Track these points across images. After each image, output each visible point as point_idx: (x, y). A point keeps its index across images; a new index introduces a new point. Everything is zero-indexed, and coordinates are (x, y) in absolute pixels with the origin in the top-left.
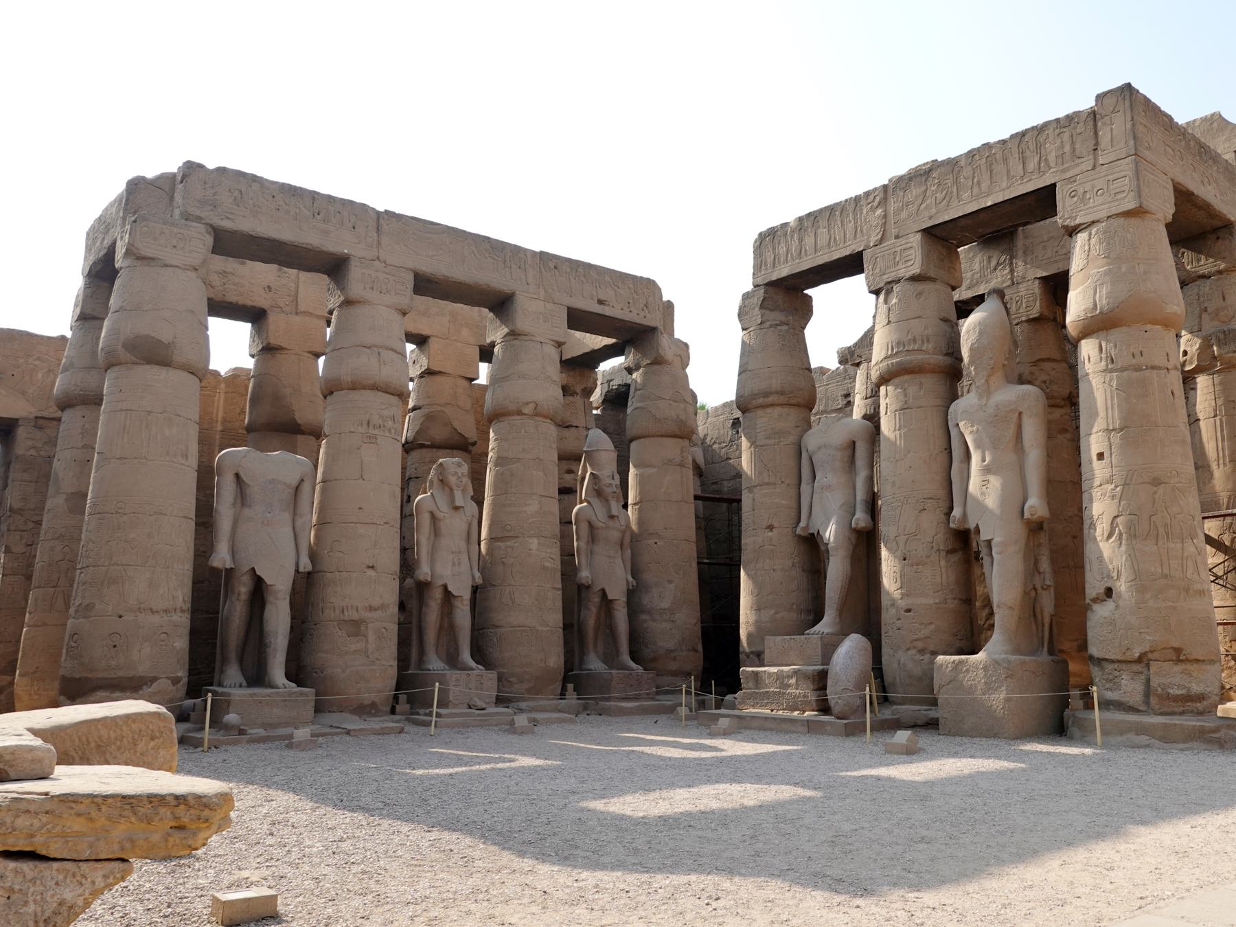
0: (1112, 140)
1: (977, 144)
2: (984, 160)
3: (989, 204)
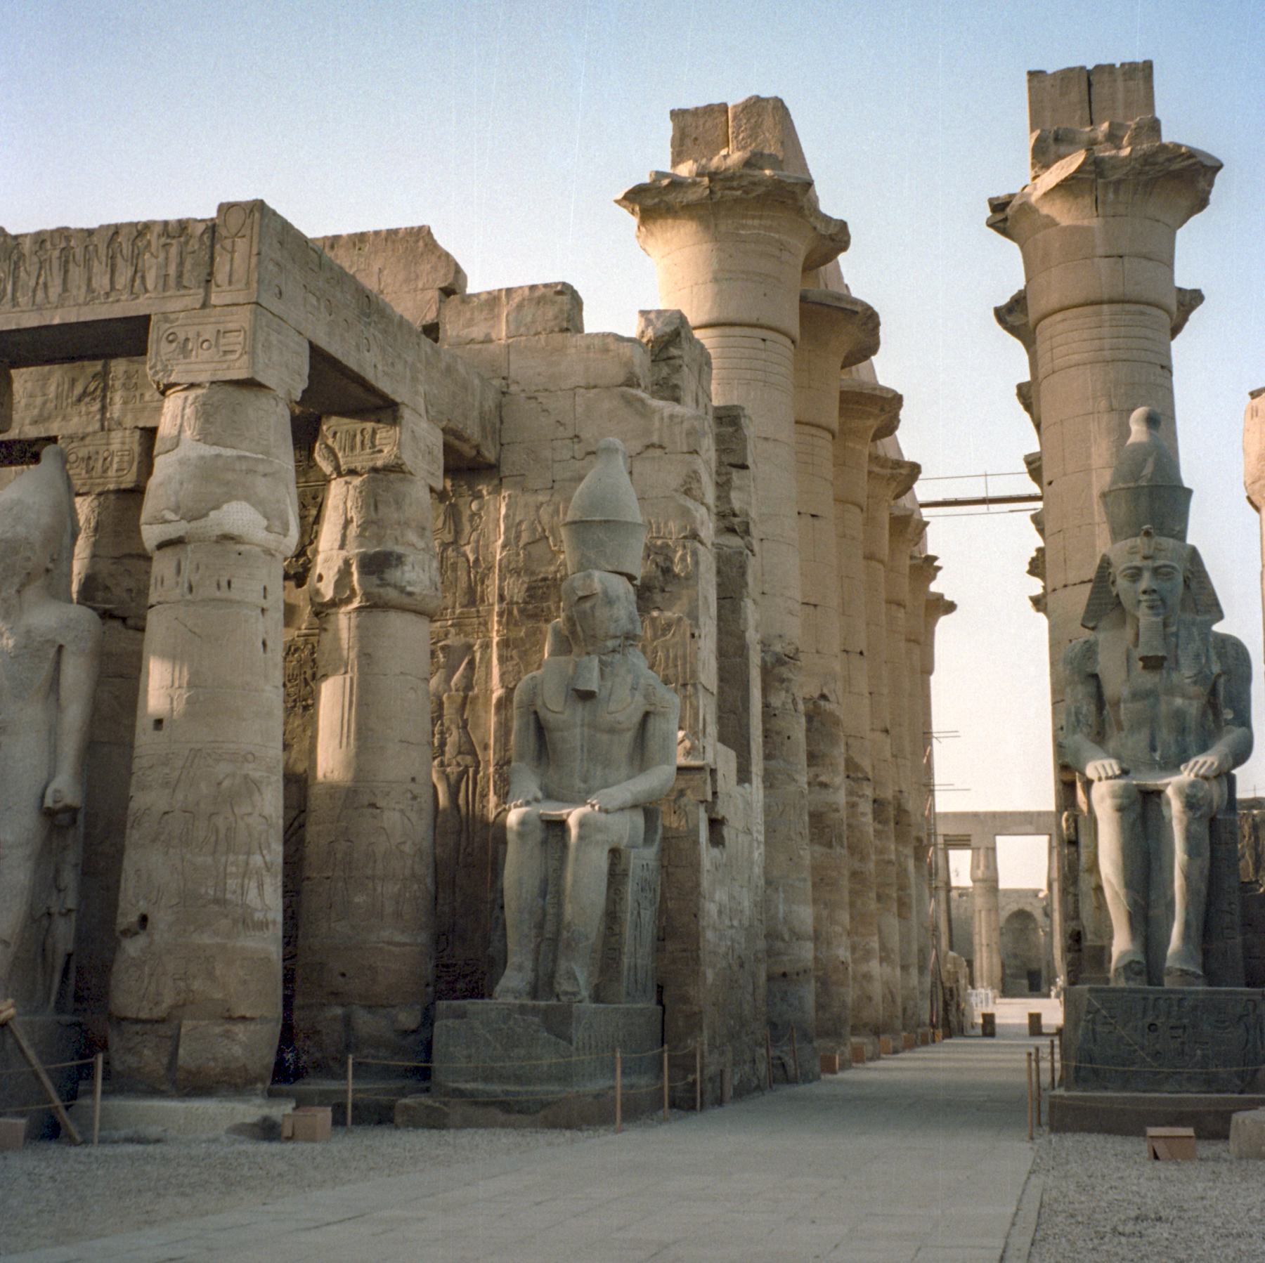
0: (231, 275)
1: (51, 225)
2: (56, 253)
3: (56, 321)
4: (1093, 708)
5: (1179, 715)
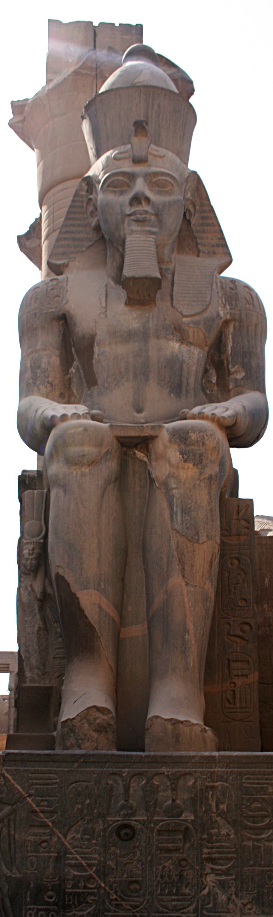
4: (56, 361)
5: (174, 365)
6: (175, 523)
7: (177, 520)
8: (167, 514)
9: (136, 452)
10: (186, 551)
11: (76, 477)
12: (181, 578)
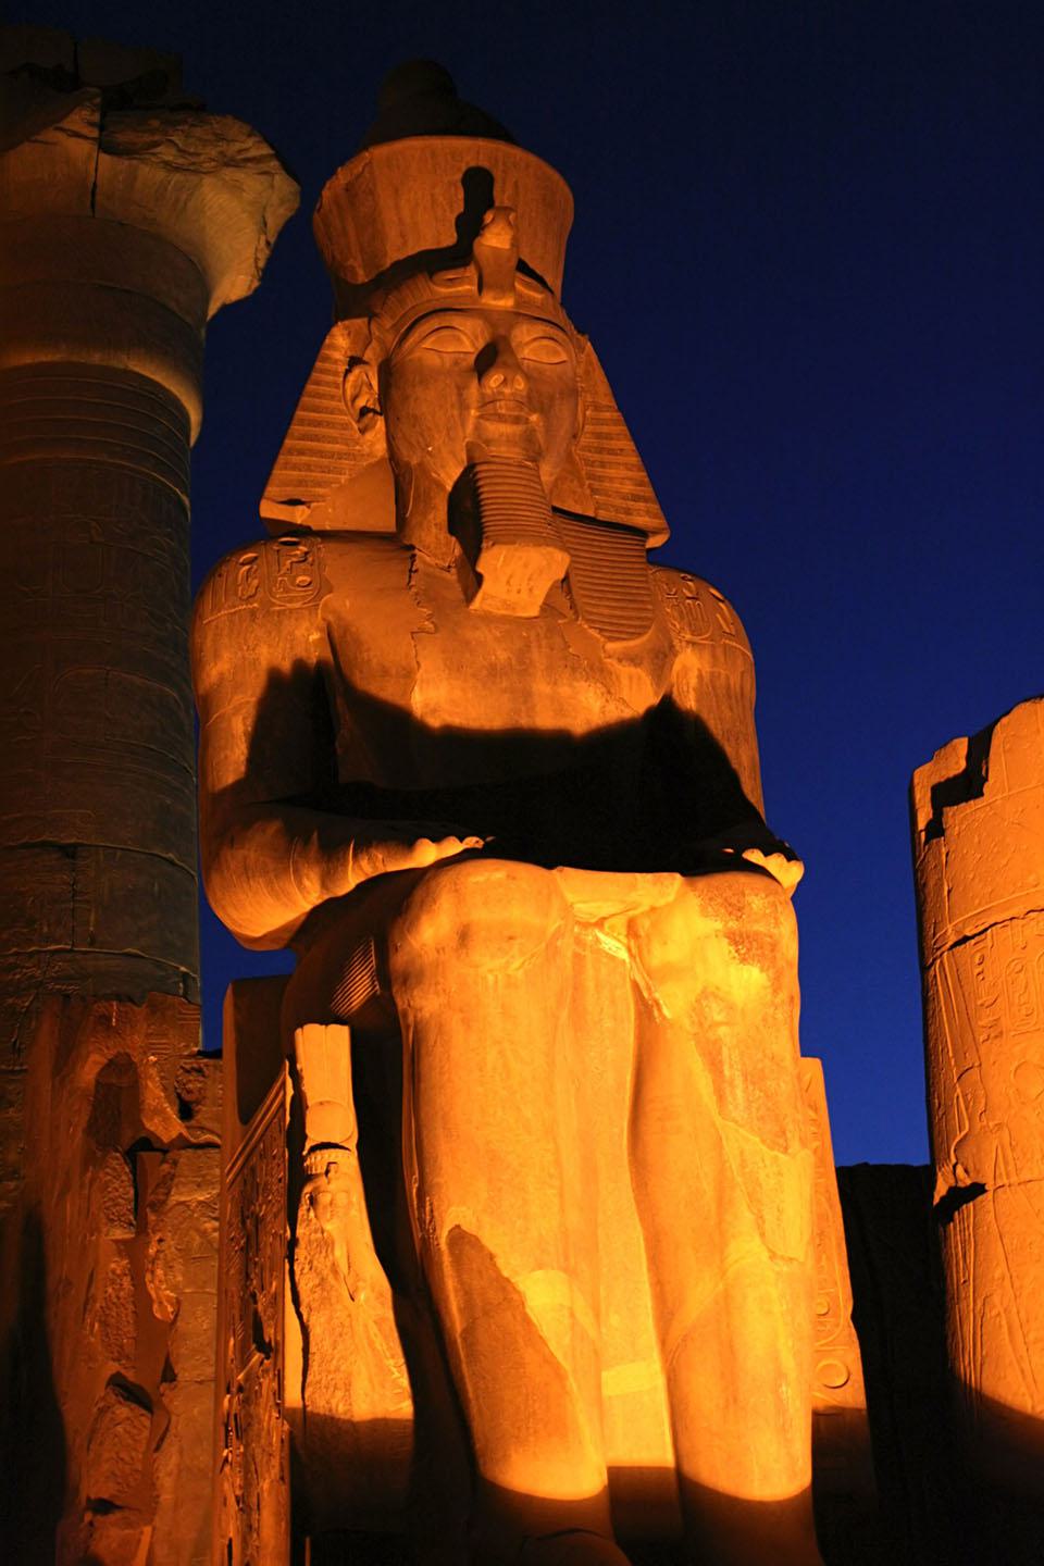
6: (731, 1107)
7: (735, 1099)
8: (704, 1083)
9: (601, 936)
10: (762, 1176)
11: (496, 990)
12: (757, 1240)
